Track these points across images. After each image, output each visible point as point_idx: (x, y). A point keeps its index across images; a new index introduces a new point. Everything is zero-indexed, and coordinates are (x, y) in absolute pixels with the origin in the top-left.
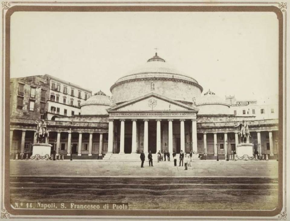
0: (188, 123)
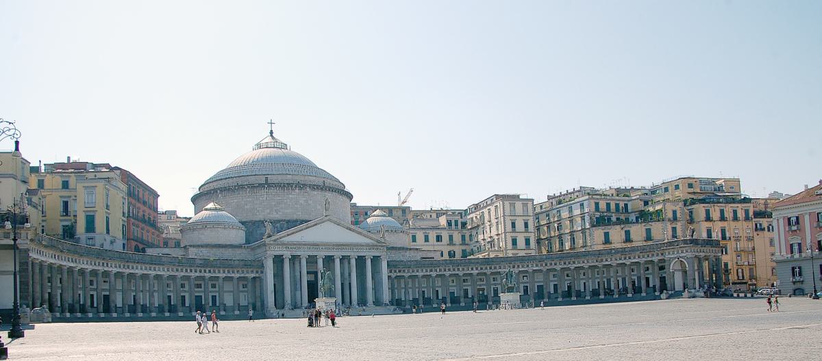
0: (376, 260)
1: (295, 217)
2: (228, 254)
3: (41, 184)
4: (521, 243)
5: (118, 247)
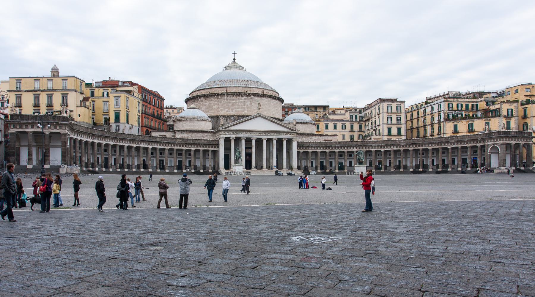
0: (289, 142)
1: (243, 114)
2: (199, 136)
3: (92, 94)
4: (394, 131)
5: (135, 131)
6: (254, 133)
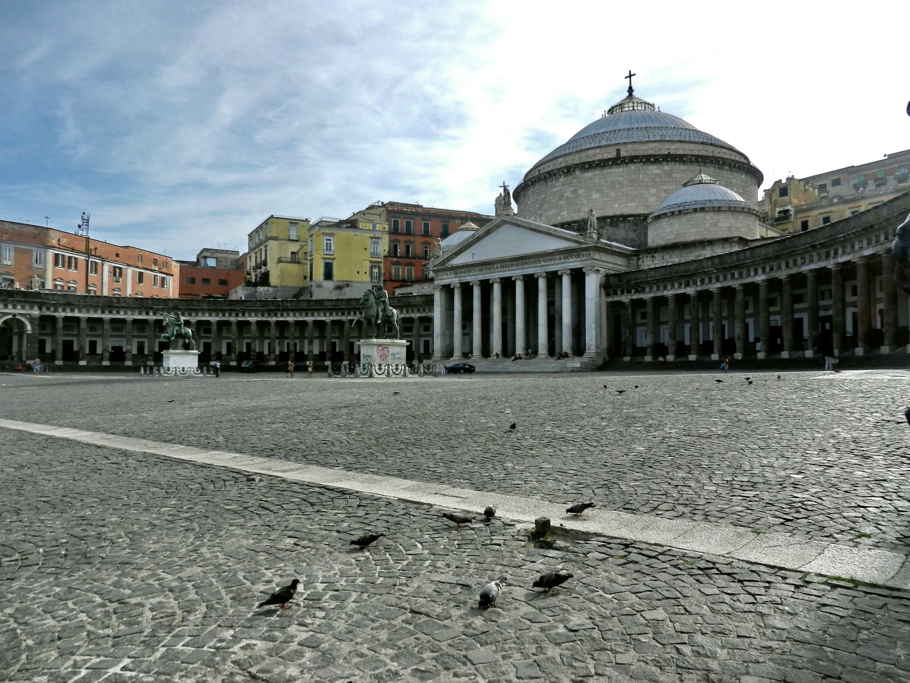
0: (578, 277)
6: (495, 266)
